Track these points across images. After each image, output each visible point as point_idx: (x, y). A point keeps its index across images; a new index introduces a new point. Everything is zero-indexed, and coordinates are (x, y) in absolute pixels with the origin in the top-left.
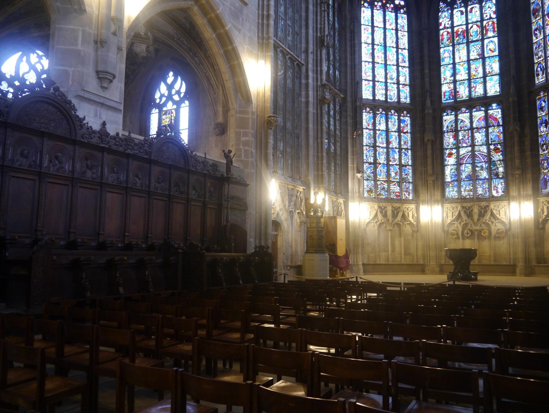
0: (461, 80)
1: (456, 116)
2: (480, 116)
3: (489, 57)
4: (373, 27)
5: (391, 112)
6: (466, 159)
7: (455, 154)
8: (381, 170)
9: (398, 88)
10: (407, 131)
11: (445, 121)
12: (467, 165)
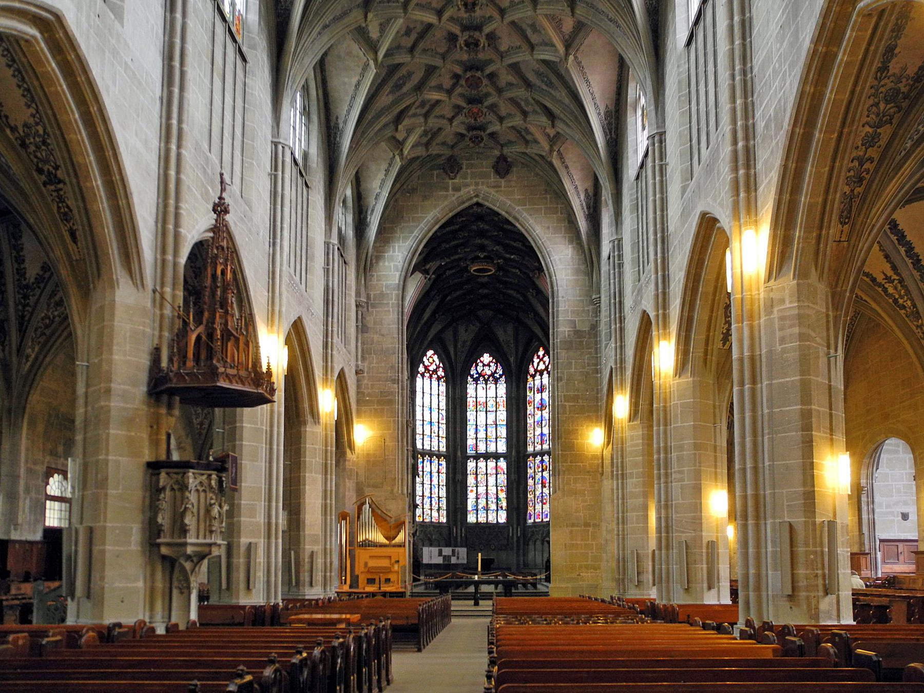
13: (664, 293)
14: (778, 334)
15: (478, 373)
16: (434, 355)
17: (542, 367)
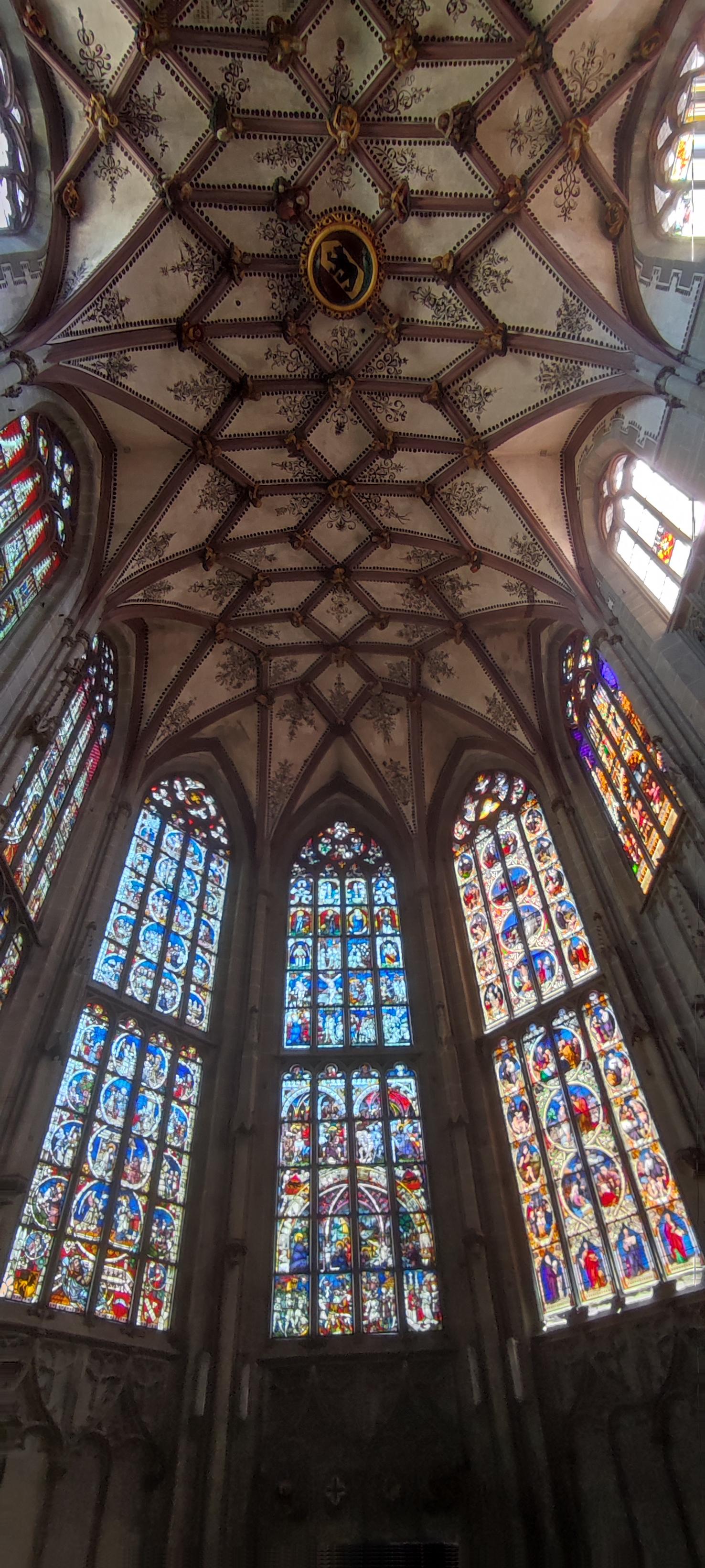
0: (328, 1006)
2: (369, 1090)
3: (386, 970)
5: (158, 1039)
6: (334, 1203)
7: (307, 1185)
8: (86, 1201)
9: (186, 989)
10: (189, 1099)
11: (286, 1092)
12: (336, 1220)
17: (489, 807)
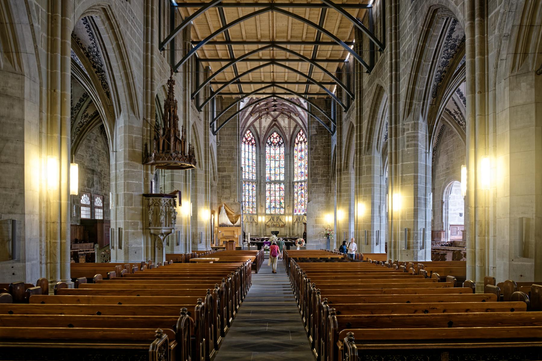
1: (270, 185)
4: (245, 151)
13: (360, 116)
14: (406, 143)
15: (271, 142)
16: (250, 133)
17: (301, 139)
